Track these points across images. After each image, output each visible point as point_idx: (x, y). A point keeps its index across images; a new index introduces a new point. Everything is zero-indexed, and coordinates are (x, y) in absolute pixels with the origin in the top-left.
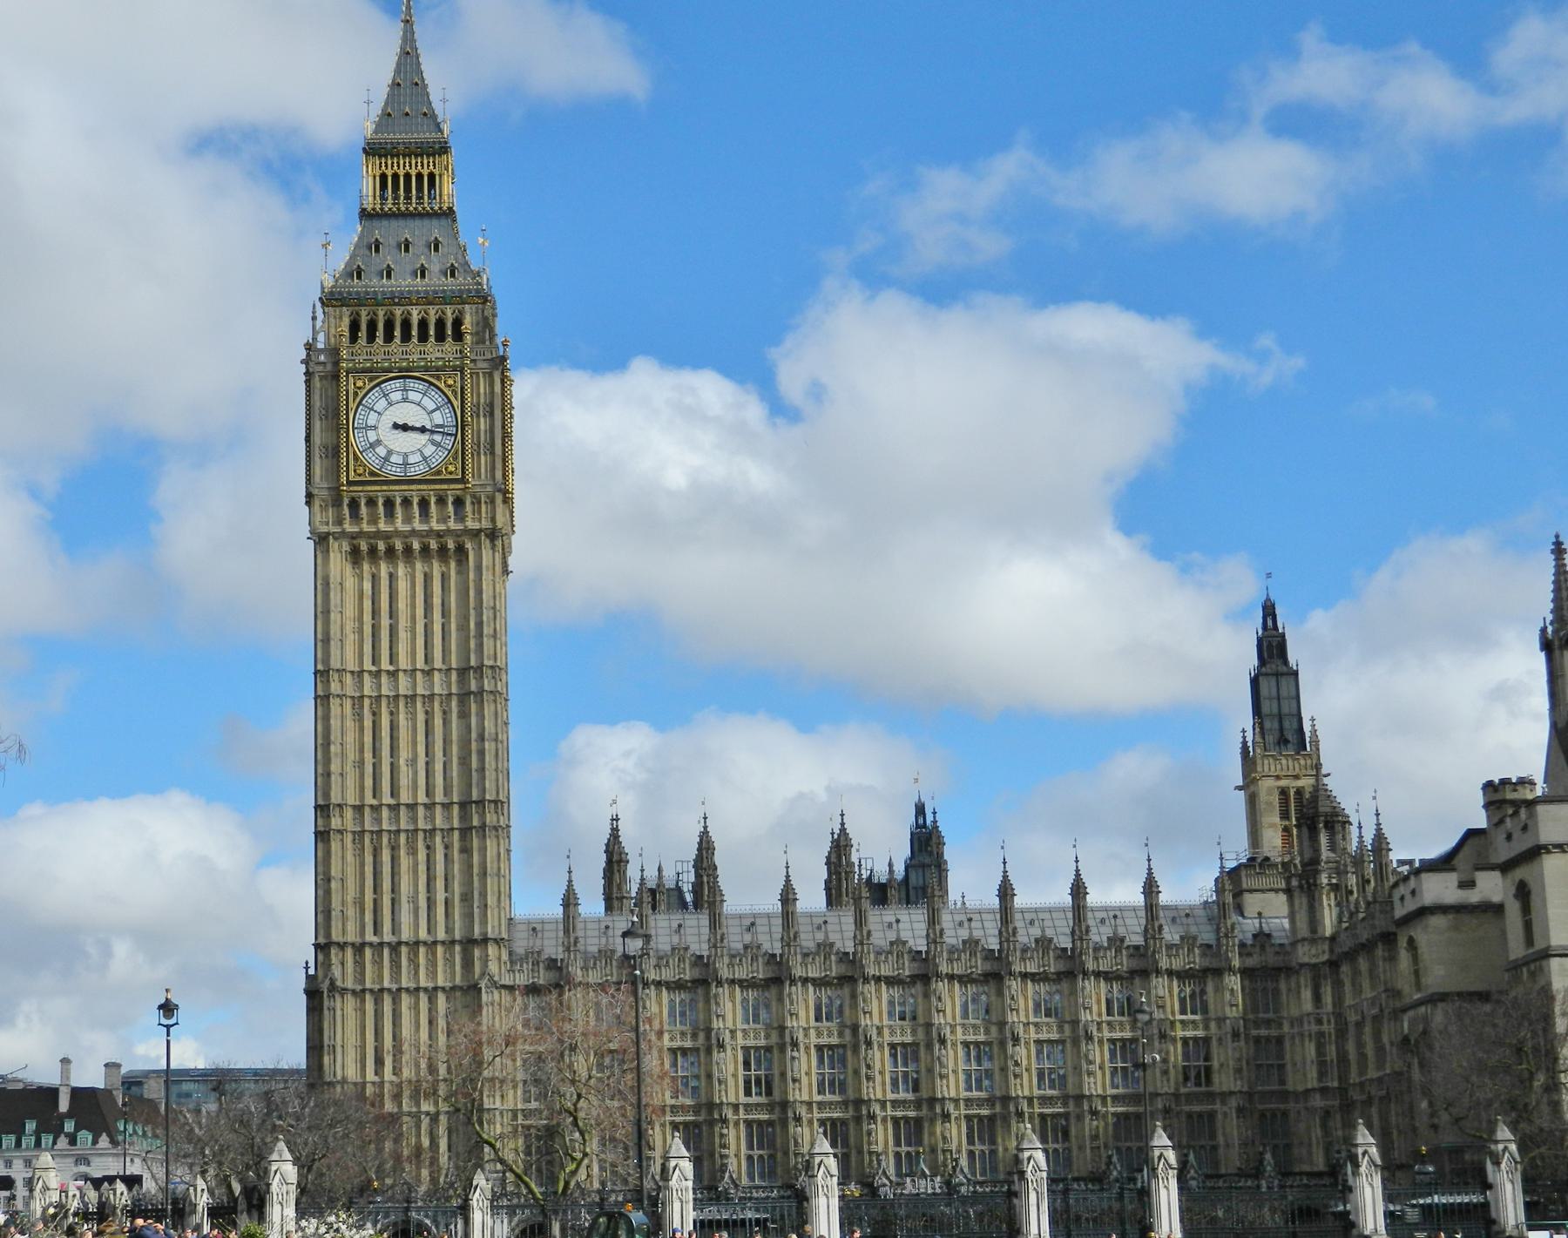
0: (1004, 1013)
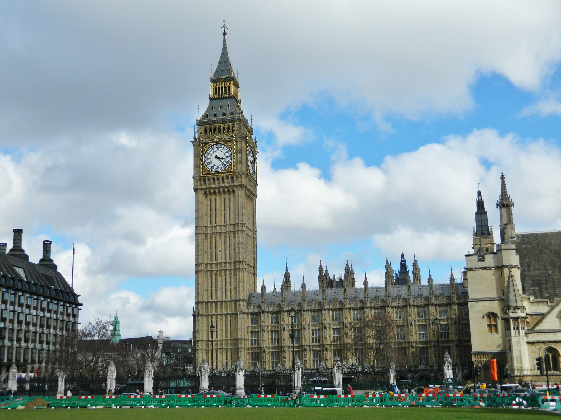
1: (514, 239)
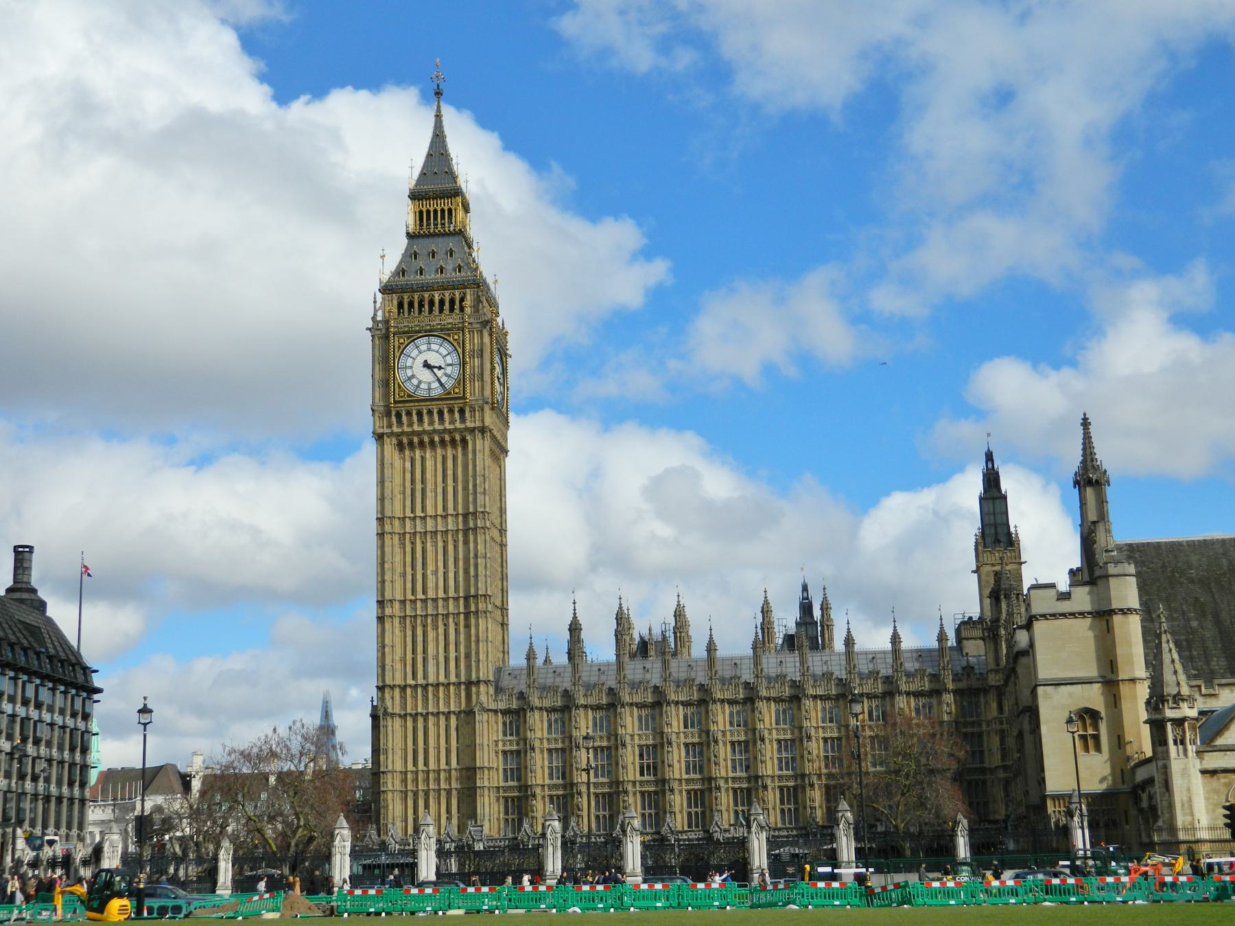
0: (801, 721)
1: (1113, 554)
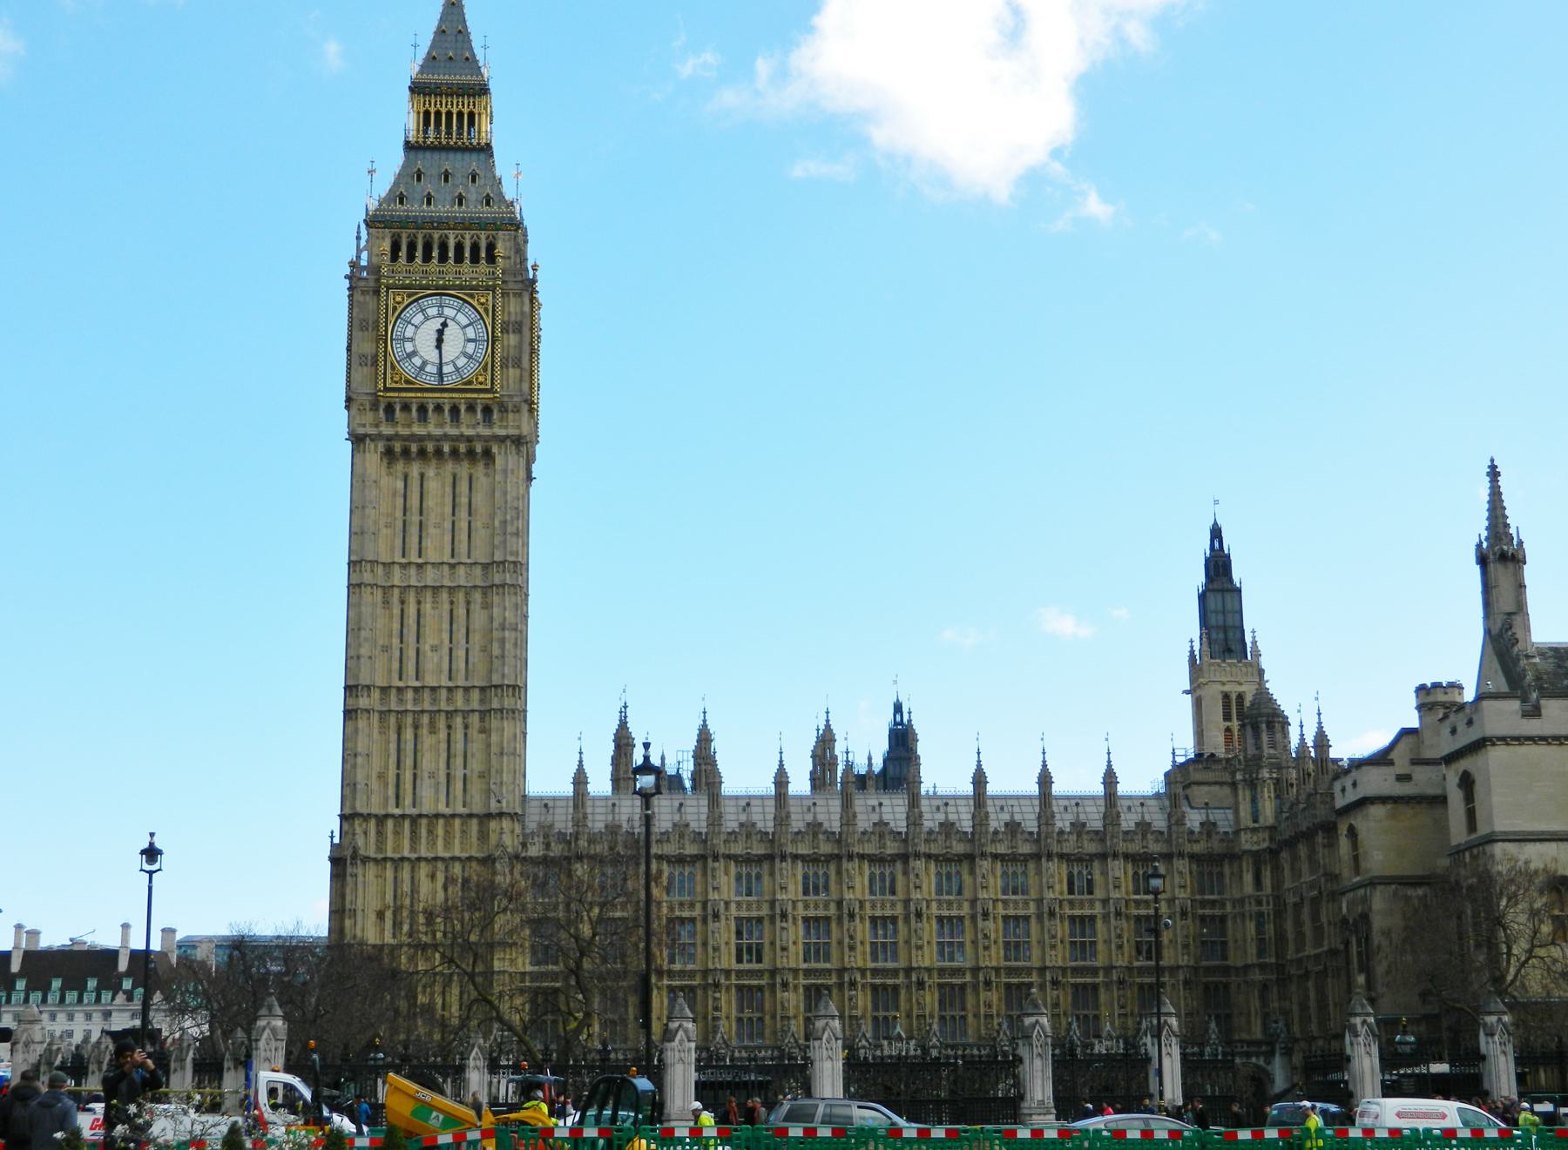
1: (1534, 660)
